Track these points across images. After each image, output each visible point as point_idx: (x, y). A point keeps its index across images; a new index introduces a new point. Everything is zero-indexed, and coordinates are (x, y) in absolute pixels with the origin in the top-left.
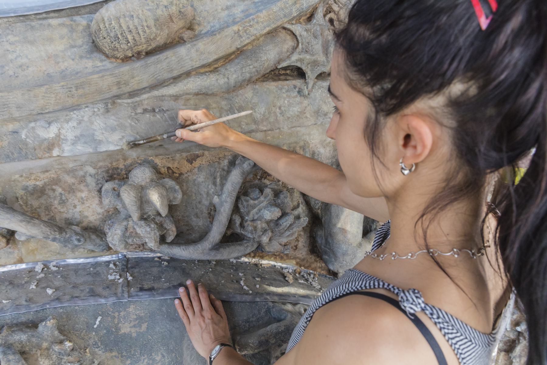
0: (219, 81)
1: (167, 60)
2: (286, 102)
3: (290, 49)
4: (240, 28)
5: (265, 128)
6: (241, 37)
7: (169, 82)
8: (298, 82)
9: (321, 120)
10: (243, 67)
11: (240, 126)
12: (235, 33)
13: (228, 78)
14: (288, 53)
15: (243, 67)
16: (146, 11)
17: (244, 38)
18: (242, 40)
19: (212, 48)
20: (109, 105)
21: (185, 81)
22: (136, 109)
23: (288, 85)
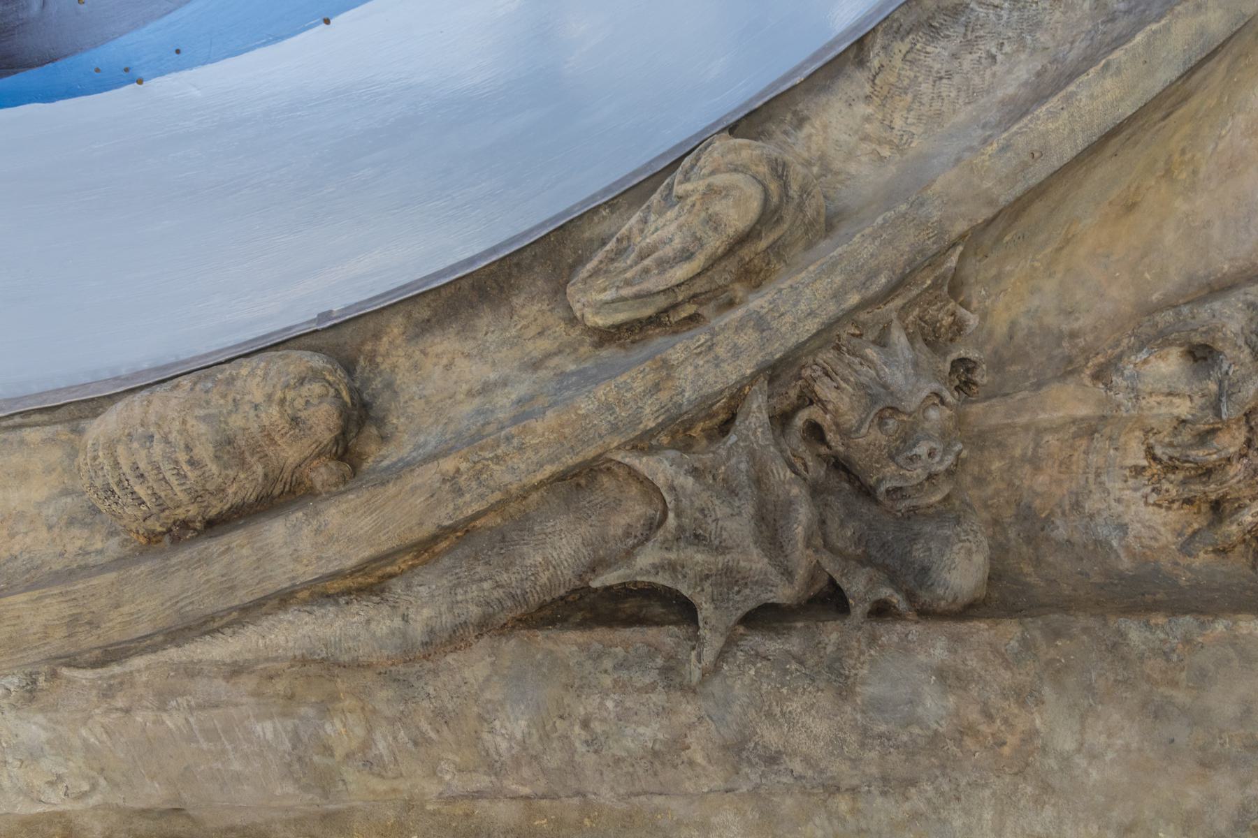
0: (373, 625)
1: (226, 559)
2: (610, 704)
4: (464, 466)
5: (526, 790)
6: (459, 492)
7: (226, 620)
8: (667, 637)
9: (755, 778)
10: (455, 586)
11: (435, 774)
12: (444, 481)
13: (405, 618)
14: (631, 542)
15: (455, 586)
16: (194, 422)
17: (468, 497)
18: (460, 501)
19: (365, 524)
20: (41, 679)
21: (266, 623)
22: (113, 697)
23: (626, 645)
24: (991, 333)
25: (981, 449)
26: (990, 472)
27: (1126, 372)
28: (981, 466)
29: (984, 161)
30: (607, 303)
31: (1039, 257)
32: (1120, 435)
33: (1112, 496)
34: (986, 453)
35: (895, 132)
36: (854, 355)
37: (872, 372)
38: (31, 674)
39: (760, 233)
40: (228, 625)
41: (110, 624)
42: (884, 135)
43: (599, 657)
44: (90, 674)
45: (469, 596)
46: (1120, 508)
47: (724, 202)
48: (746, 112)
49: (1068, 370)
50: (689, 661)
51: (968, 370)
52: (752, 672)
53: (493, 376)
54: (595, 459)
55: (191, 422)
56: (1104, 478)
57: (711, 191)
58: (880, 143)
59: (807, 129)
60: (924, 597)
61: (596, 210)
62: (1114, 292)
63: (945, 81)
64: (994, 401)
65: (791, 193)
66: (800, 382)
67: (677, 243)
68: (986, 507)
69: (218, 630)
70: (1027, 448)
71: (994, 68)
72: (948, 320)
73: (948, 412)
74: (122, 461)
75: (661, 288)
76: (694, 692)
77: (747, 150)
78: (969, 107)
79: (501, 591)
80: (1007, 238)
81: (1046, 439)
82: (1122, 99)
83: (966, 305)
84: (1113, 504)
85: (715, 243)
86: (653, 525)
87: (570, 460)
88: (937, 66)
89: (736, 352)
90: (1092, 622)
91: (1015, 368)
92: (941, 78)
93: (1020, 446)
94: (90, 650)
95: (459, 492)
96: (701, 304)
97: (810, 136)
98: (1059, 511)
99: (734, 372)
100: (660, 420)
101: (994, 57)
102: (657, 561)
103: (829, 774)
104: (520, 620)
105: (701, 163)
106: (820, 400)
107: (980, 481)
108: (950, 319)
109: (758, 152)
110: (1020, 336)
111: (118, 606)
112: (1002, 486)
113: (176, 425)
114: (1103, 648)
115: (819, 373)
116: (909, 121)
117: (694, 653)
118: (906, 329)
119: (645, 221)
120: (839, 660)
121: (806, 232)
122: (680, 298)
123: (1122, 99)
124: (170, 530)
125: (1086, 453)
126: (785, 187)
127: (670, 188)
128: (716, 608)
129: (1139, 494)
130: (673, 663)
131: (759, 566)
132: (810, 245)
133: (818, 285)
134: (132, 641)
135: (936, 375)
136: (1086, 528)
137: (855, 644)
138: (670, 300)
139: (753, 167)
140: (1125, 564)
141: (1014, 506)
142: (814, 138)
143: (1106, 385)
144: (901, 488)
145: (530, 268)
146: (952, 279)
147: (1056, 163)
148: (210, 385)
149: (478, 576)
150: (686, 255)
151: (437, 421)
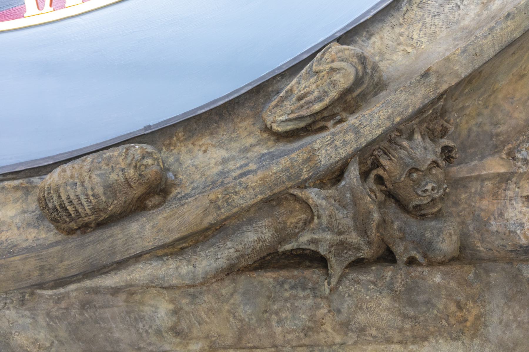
0: (179, 269)
3: (301, 224)
8: (313, 275)
13: (194, 266)
14: (297, 230)
17: (223, 210)
18: (219, 212)
20: (27, 295)
22: (60, 303)
24: (459, 135)
25: (456, 189)
26: (460, 200)
28: (456, 197)
29: (455, 57)
30: (283, 121)
31: (481, 99)
32: (520, 181)
33: (517, 210)
35: (414, 41)
36: (397, 145)
37: (406, 152)
38: (22, 293)
39: (354, 89)
40: (112, 270)
41: (59, 269)
42: (409, 42)
43: (283, 283)
44: (50, 292)
45: (224, 255)
46: (521, 216)
47: (338, 75)
48: (345, 31)
49: (496, 150)
50: (324, 285)
51: (450, 151)
52: (353, 290)
53: (227, 155)
54: (280, 193)
55: (94, 176)
56: (513, 202)
57: (332, 70)
58: (407, 45)
59: (373, 39)
60: (431, 255)
61: (274, 78)
62: (516, 115)
63: (436, 17)
64: (462, 166)
65: (368, 71)
66: (372, 157)
67: (316, 94)
68: (459, 216)
69: (107, 272)
70: (477, 188)
71: (459, 12)
72: (439, 128)
73: (440, 170)
74: (62, 195)
75: (308, 114)
76: (327, 298)
77: (349, 50)
78: (448, 30)
79: (238, 253)
80: (466, 91)
81: (486, 183)
82: (515, 30)
83: (448, 121)
85: (334, 94)
86: (307, 223)
87: (268, 193)
88: (433, 10)
89: (345, 143)
90: (506, 266)
91: (471, 150)
92: (435, 16)
93: (475, 187)
94: (49, 282)
95: (219, 208)
96: (326, 121)
97: (374, 42)
98: (492, 217)
99: (342, 154)
100: (310, 175)
101: (459, 6)
102: (310, 239)
103: (389, 335)
104: (246, 267)
105: (326, 56)
106: (382, 166)
107: (455, 204)
108: (441, 128)
109: (352, 52)
110: (473, 135)
111: (62, 262)
112: (466, 206)
113: (87, 179)
114: (511, 276)
115: (382, 153)
116: (421, 36)
117: (327, 281)
118: (421, 132)
119: (299, 83)
120: (392, 284)
121: (374, 88)
122: (317, 119)
123: (515, 30)
124: (79, 228)
125: (505, 190)
126: (365, 68)
127: (311, 68)
128: (336, 260)
130: (317, 286)
131: (356, 241)
132: (376, 94)
133: (381, 113)
134: (69, 277)
135: (435, 153)
136: (505, 225)
137: (399, 276)
138: (312, 120)
139: (351, 59)
140: (524, 241)
141: (471, 215)
142: (377, 44)
143: (513, 158)
144: (419, 205)
145: (243, 104)
146: (442, 109)
147: (486, 58)
148: (100, 160)
149: (227, 247)
150: (319, 99)
151: (201, 177)
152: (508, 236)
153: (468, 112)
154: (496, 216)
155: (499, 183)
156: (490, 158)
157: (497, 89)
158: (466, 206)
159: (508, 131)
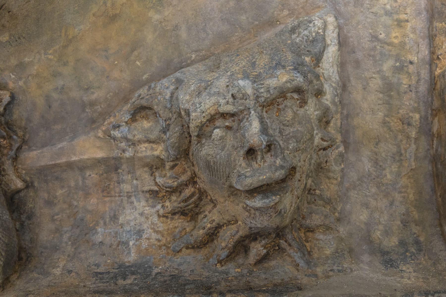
26: (56, 197)
27: (121, 128)
34: (50, 184)
46: (143, 219)
56: (133, 199)
62: (116, 74)
64: (45, 149)
84: (137, 216)
91: (58, 127)
98: (102, 222)
129: (155, 209)
136: (116, 233)
152: (115, 249)
153: (34, 72)
154: (107, 220)
155: (106, 173)
156: (83, 137)
157: (73, 37)
158: (65, 206)
159: (107, 98)
